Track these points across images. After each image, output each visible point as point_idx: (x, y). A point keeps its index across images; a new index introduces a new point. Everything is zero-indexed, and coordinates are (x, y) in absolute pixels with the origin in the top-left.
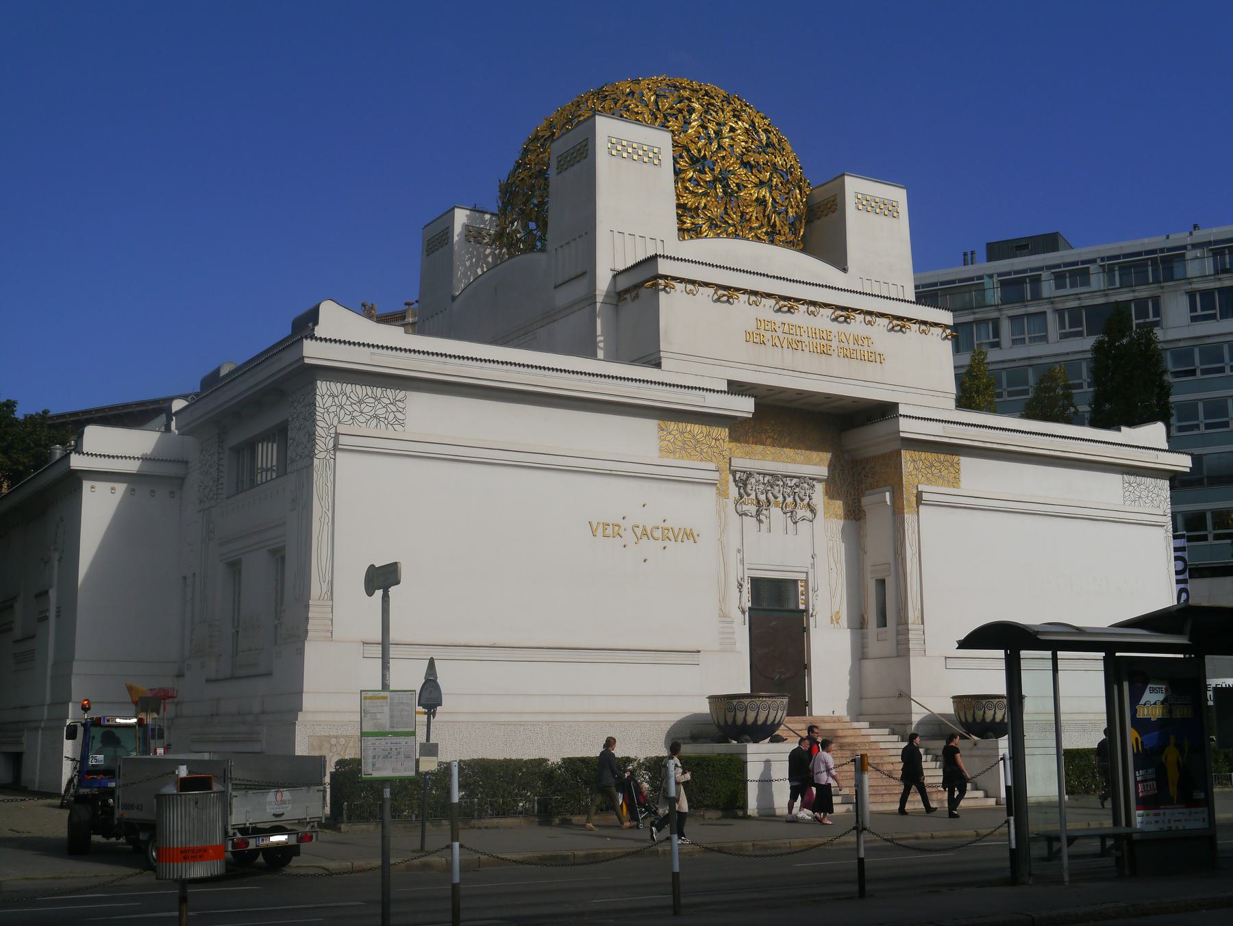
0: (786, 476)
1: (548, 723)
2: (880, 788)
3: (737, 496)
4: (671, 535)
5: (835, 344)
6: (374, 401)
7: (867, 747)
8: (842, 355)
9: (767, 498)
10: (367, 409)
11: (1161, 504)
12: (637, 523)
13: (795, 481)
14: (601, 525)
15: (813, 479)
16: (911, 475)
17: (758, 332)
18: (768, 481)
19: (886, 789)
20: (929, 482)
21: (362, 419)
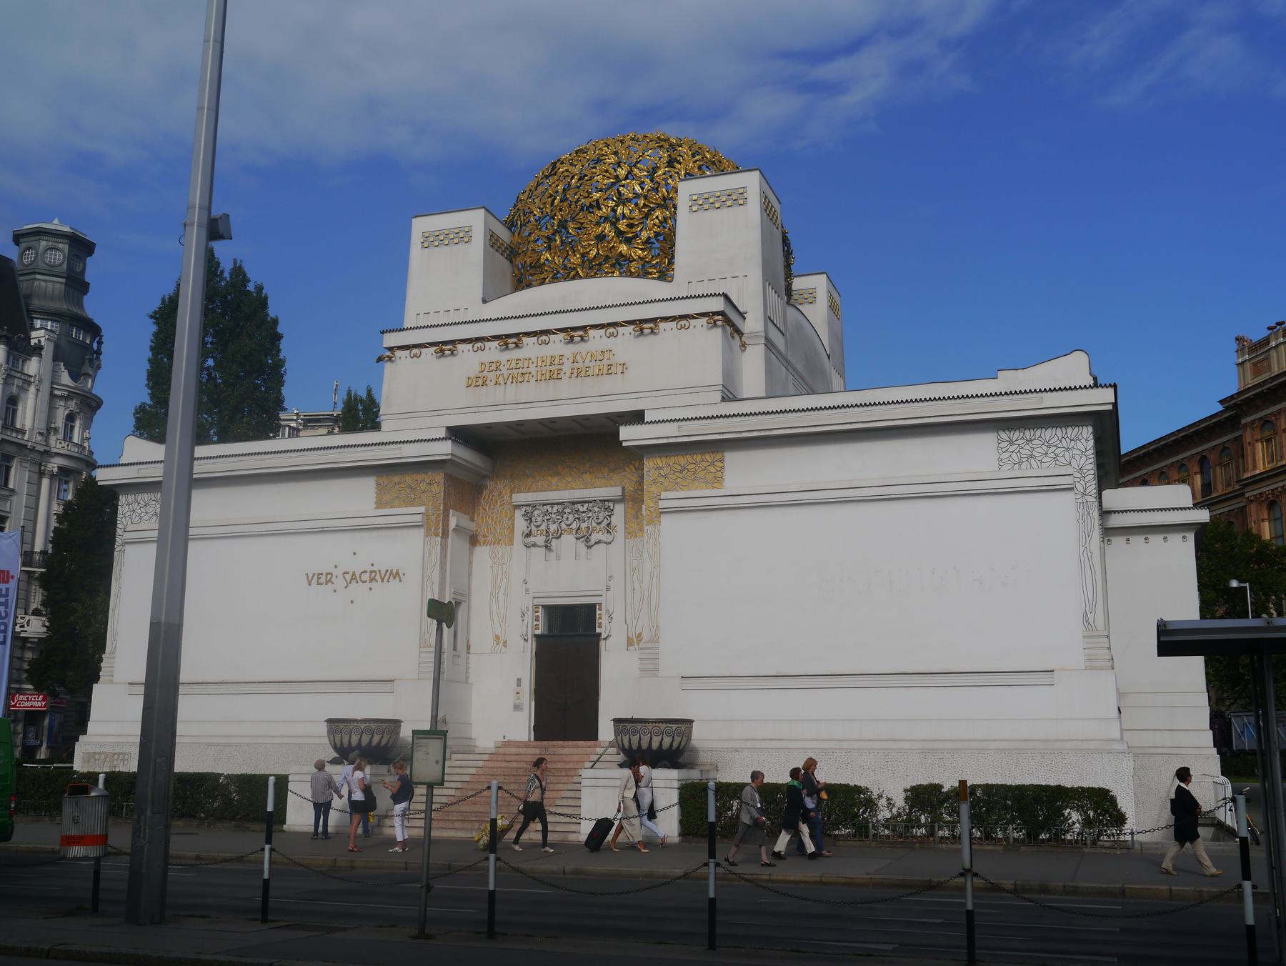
0: (574, 503)
1: (248, 745)
2: (468, 814)
4: (378, 577)
5: (566, 368)
6: (155, 502)
7: (563, 774)
8: (575, 374)
10: (151, 509)
11: (1074, 463)
12: (347, 571)
14: (316, 577)
15: (609, 501)
16: (655, 483)
19: (476, 816)
20: (677, 486)
21: (146, 518)
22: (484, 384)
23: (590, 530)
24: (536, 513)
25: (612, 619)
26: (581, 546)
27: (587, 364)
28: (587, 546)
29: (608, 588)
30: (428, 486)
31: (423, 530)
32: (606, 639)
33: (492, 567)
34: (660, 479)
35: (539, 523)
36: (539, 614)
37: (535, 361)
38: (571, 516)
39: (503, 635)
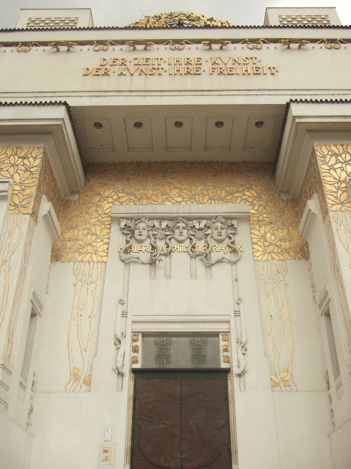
3: (125, 242)
9: (166, 244)
13: (204, 223)
15: (232, 218)
16: (335, 170)
17: (101, 67)
18: (167, 226)
22: (106, 74)
23: (210, 248)
24: (141, 225)
25: (246, 350)
26: (200, 267)
27: (229, 65)
28: (206, 267)
29: (237, 314)
30: (20, 160)
31: (7, 204)
32: (239, 375)
33: (75, 285)
34: (340, 165)
35: (143, 237)
36: (139, 343)
37: (167, 61)
38: (185, 232)
39: (86, 367)
